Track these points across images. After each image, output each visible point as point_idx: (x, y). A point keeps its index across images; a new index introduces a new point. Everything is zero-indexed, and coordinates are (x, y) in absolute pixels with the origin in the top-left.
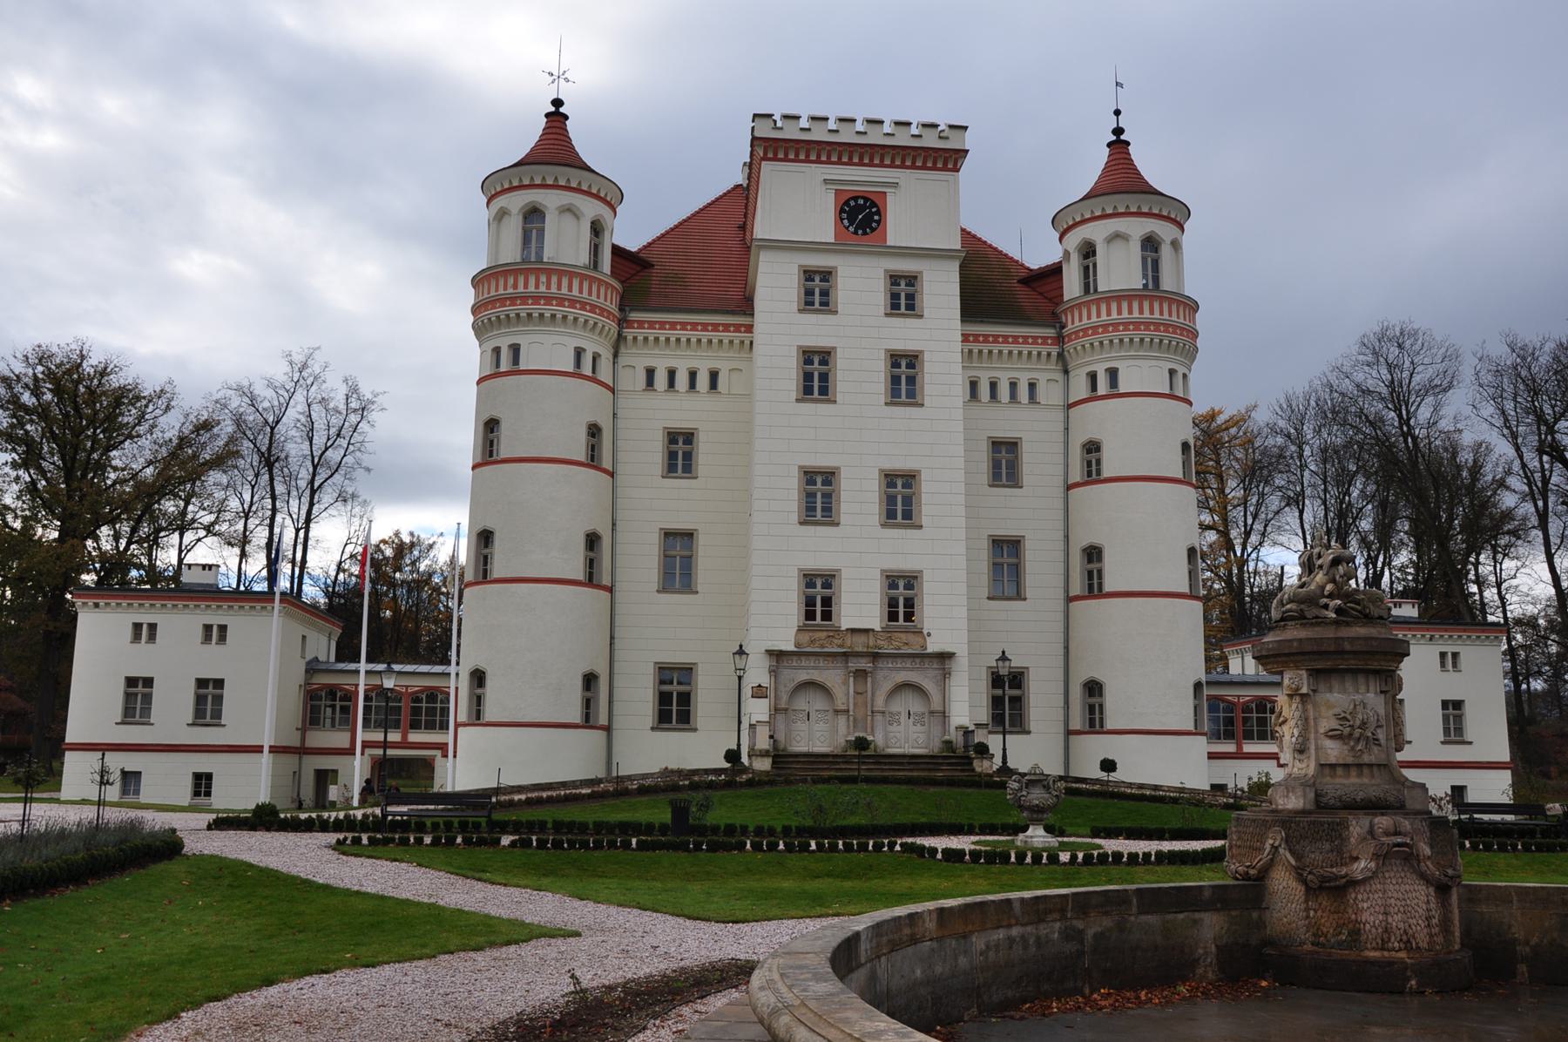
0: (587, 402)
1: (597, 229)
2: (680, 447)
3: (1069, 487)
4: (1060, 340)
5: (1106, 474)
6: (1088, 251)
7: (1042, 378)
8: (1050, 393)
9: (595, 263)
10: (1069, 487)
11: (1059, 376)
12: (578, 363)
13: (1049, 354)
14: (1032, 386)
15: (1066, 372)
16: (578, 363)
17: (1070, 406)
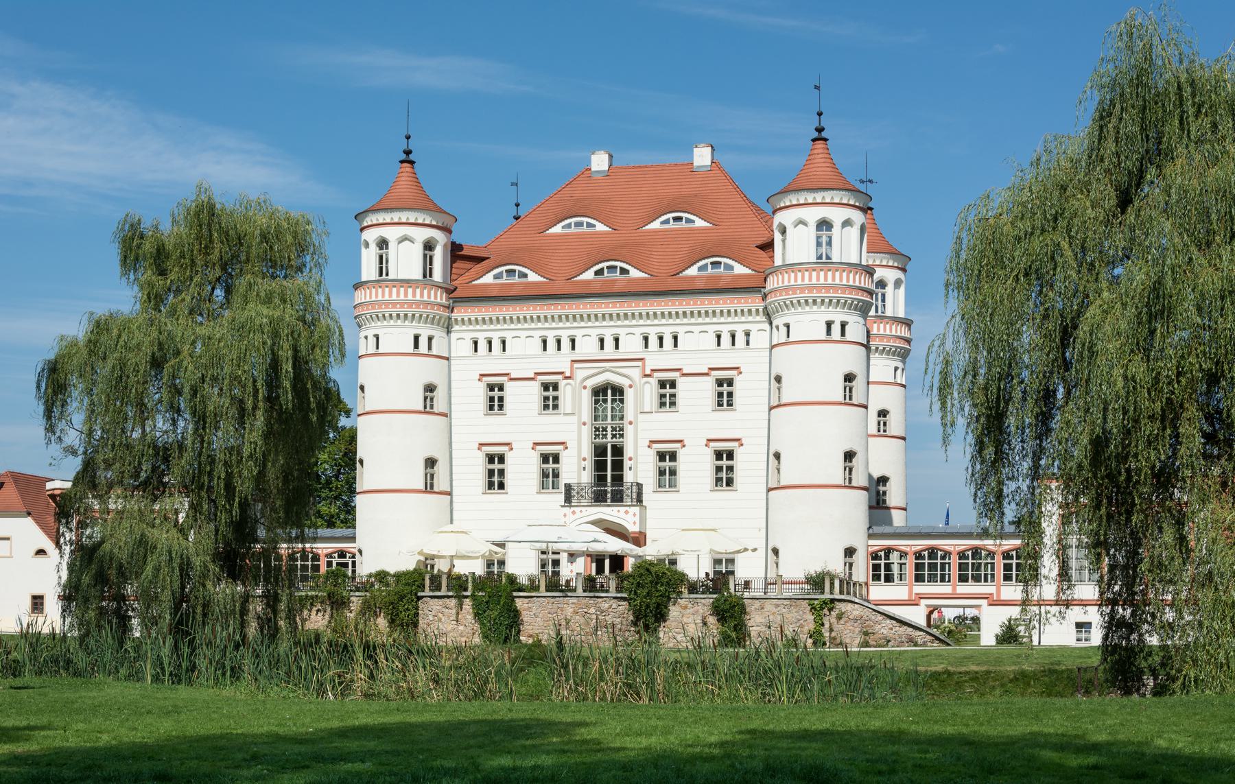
0: (427, 370)
1: (429, 246)
2: (496, 393)
3: (771, 408)
4: (765, 297)
5: (784, 401)
6: (783, 231)
7: (753, 328)
8: (761, 338)
9: (428, 272)
10: (771, 408)
11: (767, 326)
12: (416, 346)
13: (757, 310)
14: (747, 334)
15: (771, 324)
16: (416, 346)
17: (773, 347)
